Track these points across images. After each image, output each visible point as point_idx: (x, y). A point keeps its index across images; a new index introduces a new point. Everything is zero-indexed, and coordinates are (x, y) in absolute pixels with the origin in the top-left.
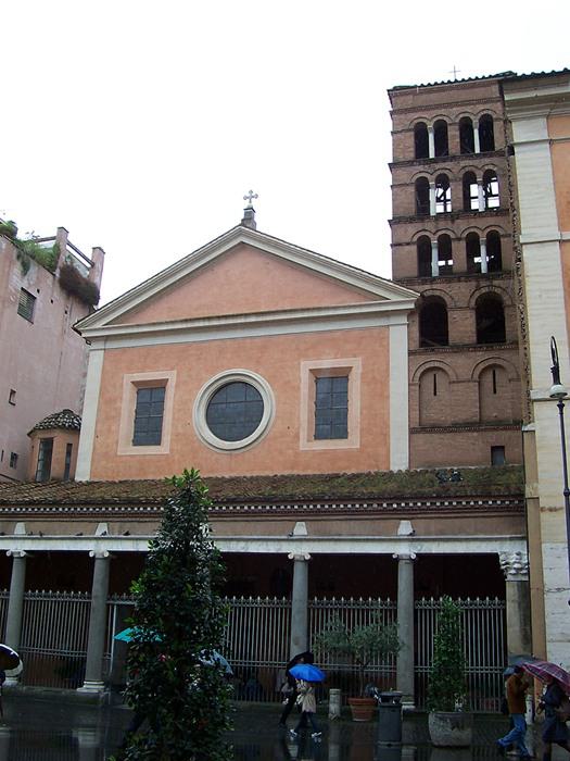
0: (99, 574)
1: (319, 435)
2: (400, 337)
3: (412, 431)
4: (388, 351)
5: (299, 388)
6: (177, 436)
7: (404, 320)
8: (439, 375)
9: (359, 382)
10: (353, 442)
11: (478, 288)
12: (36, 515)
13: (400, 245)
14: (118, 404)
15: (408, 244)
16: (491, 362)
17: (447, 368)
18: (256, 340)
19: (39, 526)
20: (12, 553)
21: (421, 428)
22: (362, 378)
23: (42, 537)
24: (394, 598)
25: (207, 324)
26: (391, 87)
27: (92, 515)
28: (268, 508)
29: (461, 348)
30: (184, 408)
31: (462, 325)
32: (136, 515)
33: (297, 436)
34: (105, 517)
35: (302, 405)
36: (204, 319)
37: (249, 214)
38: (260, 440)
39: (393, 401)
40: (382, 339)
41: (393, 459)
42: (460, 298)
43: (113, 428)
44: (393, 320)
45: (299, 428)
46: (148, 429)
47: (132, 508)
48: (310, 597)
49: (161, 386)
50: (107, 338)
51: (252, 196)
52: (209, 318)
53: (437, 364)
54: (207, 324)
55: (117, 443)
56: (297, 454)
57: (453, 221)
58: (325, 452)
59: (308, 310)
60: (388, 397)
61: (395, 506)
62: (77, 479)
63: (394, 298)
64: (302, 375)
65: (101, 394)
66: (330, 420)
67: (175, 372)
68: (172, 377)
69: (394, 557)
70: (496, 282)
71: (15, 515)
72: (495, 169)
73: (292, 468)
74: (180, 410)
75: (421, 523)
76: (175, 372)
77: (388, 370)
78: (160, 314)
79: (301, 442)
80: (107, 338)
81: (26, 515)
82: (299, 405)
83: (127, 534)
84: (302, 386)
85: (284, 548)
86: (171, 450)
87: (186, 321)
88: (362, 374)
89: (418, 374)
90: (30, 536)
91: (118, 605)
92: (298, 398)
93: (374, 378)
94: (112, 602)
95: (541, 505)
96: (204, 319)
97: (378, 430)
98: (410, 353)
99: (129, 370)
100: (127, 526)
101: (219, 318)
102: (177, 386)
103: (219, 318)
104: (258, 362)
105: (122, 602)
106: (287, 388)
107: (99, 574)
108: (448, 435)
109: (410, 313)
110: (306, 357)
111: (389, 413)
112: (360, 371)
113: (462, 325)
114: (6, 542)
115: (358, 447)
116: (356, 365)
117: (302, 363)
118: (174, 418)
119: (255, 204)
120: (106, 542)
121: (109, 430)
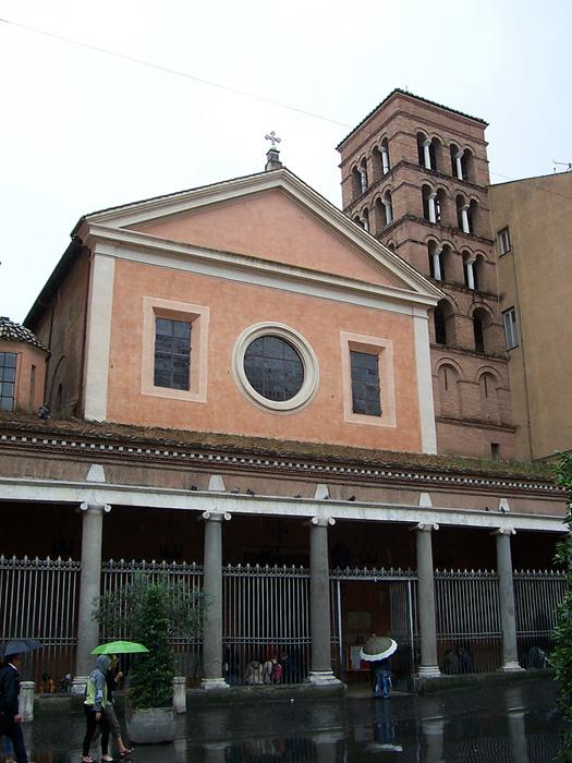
1: (356, 410)
2: (423, 329)
3: (438, 420)
4: (414, 339)
5: (340, 359)
6: (214, 385)
7: (425, 315)
8: (448, 370)
9: (392, 364)
10: (388, 421)
11: (474, 302)
12: (240, 468)
14: (138, 331)
15: (422, 244)
17: (457, 368)
18: (295, 296)
19: (244, 482)
20: (211, 515)
22: (394, 361)
23: (251, 495)
25: (249, 264)
26: (402, 88)
27: (314, 474)
29: (465, 352)
30: (220, 354)
31: (464, 331)
33: (341, 407)
34: (326, 478)
36: (248, 258)
37: (273, 157)
39: (420, 387)
40: (409, 329)
41: (424, 444)
42: (462, 303)
43: (134, 359)
44: (417, 312)
45: (342, 399)
46: (173, 367)
47: (360, 471)
48: (224, 564)
49: (187, 321)
51: (272, 138)
52: (253, 259)
53: (450, 362)
54: (249, 264)
55: (140, 379)
56: (342, 425)
57: (452, 235)
59: (352, 280)
60: (416, 383)
62: (89, 416)
63: (421, 292)
65: (115, 313)
66: (366, 400)
70: (485, 301)
71: (210, 465)
74: (216, 355)
78: (183, 233)
83: (353, 499)
85: (409, 517)
87: (228, 254)
88: (394, 356)
90: (234, 495)
92: (340, 367)
93: (403, 363)
94: (334, 578)
96: (248, 258)
97: (409, 412)
98: (432, 347)
99: (151, 290)
100: (350, 491)
101: (264, 261)
103: (264, 261)
104: (298, 320)
105: (345, 578)
106: (329, 354)
108: (462, 428)
109: (430, 309)
110: (345, 328)
113: (464, 331)
114: (198, 499)
116: (389, 346)
118: (209, 362)
119: (278, 147)
120: (330, 508)
121: (128, 361)
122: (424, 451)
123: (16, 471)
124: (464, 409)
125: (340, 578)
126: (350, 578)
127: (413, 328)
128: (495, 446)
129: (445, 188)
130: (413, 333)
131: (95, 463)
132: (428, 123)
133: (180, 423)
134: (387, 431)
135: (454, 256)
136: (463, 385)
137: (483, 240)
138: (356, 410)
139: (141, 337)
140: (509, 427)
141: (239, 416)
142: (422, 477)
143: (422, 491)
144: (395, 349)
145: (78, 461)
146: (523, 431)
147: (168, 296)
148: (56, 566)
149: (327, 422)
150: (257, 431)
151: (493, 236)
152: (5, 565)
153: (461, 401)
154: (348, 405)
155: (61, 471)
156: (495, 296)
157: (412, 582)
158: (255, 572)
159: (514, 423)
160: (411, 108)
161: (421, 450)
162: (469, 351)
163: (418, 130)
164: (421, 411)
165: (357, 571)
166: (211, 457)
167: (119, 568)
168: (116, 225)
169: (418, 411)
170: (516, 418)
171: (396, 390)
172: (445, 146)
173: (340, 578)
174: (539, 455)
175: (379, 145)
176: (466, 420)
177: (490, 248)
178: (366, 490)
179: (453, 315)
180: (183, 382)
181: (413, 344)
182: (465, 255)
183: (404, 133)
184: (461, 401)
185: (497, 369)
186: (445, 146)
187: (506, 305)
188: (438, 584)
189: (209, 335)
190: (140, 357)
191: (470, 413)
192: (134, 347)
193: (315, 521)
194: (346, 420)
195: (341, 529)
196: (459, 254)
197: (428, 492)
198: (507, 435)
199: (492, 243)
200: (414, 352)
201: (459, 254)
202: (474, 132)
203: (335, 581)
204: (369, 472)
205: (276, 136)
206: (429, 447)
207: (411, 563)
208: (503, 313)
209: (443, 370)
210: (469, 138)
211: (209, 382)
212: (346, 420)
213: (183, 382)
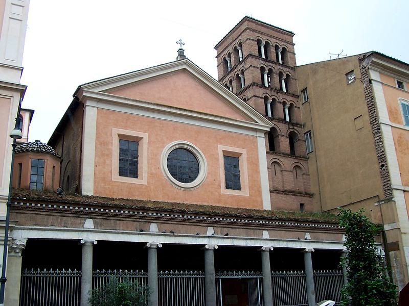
0: (210, 259)
1: (227, 187)
2: (262, 143)
3: (270, 192)
5: (218, 160)
6: (151, 175)
8: (276, 165)
10: (245, 192)
11: (289, 129)
12: (166, 219)
13: (258, 97)
14: (110, 147)
15: (261, 98)
16: (297, 164)
17: (281, 163)
18: (195, 127)
19: (168, 227)
20: (151, 245)
21: (273, 191)
22: (248, 160)
23: (172, 234)
25: (169, 110)
27: (205, 222)
29: (285, 155)
30: (154, 158)
32: (231, 224)
33: (219, 186)
34: (213, 224)
35: (220, 169)
36: (168, 107)
37: (181, 53)
38: (200, 185)
40: (255, 144)
42: (283, 129)
43: (108, 162)
44: (259, 134)
45: (220, 181)
46: (129, 166)
47: (230, 220)
48: (159, 271)
49: (136, 141)
50: (100, 101)
51: (180, 43)
52: (171, 107)
53: (277, 161)
54: (169, 110)
56: (220, 195)
58: (234, 196)
59: (224, 118)
60: (259, 172)
62: (84, 193)
63: (261, 123)
66: (233, 182)
68: (145, 136)
70: (295, 128)
72: (290, 75)
74: (152, 159)
78: (133, 94)
80: (100, 101)
81: (158, 219)
83: (227, 235)
84: (220, 158)
87: (157, 105)
88: (248, 158)
92: (219, 165)
93: (252, 161)
94: (218, 277)
95: (402, 231)
96: (168, 107)
98: (267, 153)
99: (116, 125)
100: (226, 230)
101: (177, 108)
102: (149, 143)
103: (177, 108)
104: (196, 140)
105: (224, 277)
106: (212, 158)
107: (210, 259)
109: (266, 133)
110: (221, 143)
114: (144, 236)
116: (244, 152)
118: (148, 163)
120: (215, 239)
121: (105, 163)
122: (264, 208)
123: (45, 223)
124: (285, 186)
126: (226, 277)
127: (257, 143)
128: (302, 205)
129: (273, 68)
130: (257, 145)
131: (88, 218)
132: (262, 33)
133: (134, 196)
134: (244, 198)
135: (278, 104)
136: (284, 173)
137: (293, 95)
138: (227, 187)
140: (309, 194)
143: (264, 230)
144: (248, 155)
145: (79, 217)
146: (317, 197)
147: (126, 128)
148: (68, 274)
149: (212, 193)
150: (174, 199)
151: (299, 93)
152: (59, 274)
153: (283, 182)
154: (223, 184)
155: (70, 223)
156: (301, 125)
157: (259, 278)
158: (176, 275)
159: (312, 193)
160: (254, 26)
161: (263, 208)
162: (288, 155)
163: (258, 38)
164: (262, 187)
165: (230, 273)
166: (150, 214)
167: (102, 274)
168: (97, 90)
169: (260, 187)
170: (313, 189)
171: (248, 176)
172: (273, 46)
173: (221, 277)
174: (325, 209)
175: (239, 73)
176: (286, 191)
177: (297, 99)
178: (234, 230)
179: (278, 136)
180: (134, 174)
182: (284, 104)
183: (250, 39)
184: (283, 182)
185: (302, 163)
186: (273, 46)
187: (306, 130)
188: (273, 278)
189: (148, 149)
190: (112, 161)
191: (288, 187)
192: (107, 155)
193: (207, 247)
194: (222, 193)
195: (221, 252)
196: (280, 103)
198: (308, 198)
199: (298, 97)
201: (280, 103)
202: (287, 38)
203: (219, 279)
204: (235, 220)
205: (182, 42)
206: (267, 206)
207: (259, 268)
208: (305, 134)
209: (273, 165)
210: (285, 41)
211: (148, 173)
212: (222, 193)
213: (134, 174)
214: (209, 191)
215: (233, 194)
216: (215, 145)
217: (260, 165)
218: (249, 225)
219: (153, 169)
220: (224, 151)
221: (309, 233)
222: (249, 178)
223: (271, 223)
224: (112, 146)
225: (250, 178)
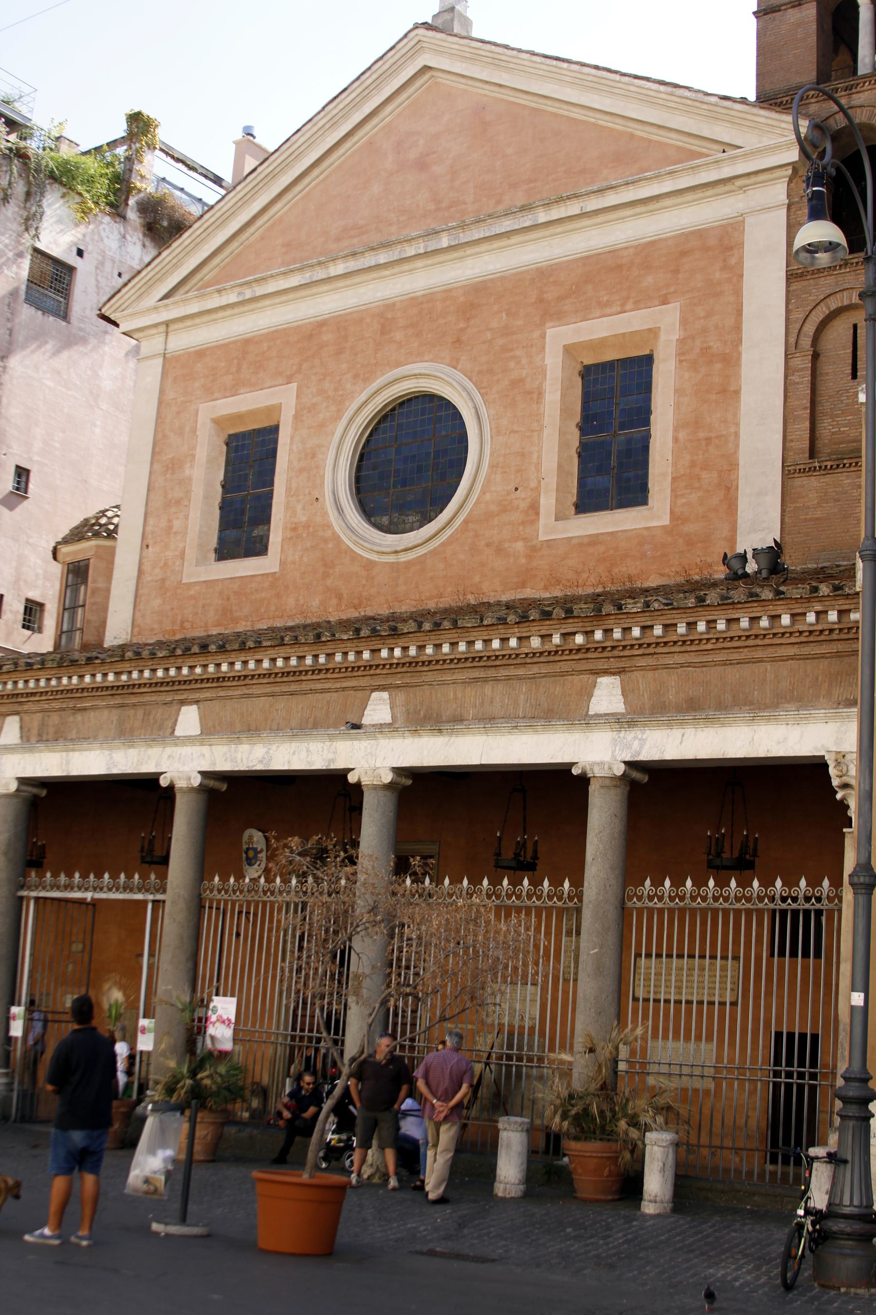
5: (540, 394)
9: (672, 365)
24: (578, 882)
28: (309, 661)
33: (534, 508)
35: (546, 432)
43: (177, 524)
45: (537, 490)
56: (533, 550)
60: (737, 392)
61: (579, 639)
64: (548, 361)
67: (294, 385)
69: (575, 771)
73: (523, 585)
74: (301, 470)
75: (643, 680)
76: (294, 385)
77: (738, 328)
79: (542, 521)
82: (541, 430)
86: (282, 563)
88: (682, 341)
89: (810, 329)
91: (37, 899)
99: (209, 393)
111: (737, 435)
112: (675, 336)
115: (666, 521)
117: (549, 332)
125: (34, 894)
133: (235, 620)
139: (190, 479)
141: (329, 582)
142: (172, 672)
143: (183, 703)
144: (684, 322)
147: (233, 390)
149: (500, 551)
165: (63, 878)
169: (734, 466)
171: (676, 429)
173: (34, 894)
178: (79, 717)
181: (738, 292)
189: (292, 438)
190: (187, 517)
192: (178, 502)
194: (542, 537)
197: (197, 702)
200: (739, 312)
214: (488, 545)
215: (592, 531)
216: (536, 334)
217: (744, 357)
218: (130, 688)
219: (299, 508)
220: (569, 350)
221: (385, 695)
222: (676, 440)
223: (198, 670)
224: (192, 467)
225: (682, 435)
